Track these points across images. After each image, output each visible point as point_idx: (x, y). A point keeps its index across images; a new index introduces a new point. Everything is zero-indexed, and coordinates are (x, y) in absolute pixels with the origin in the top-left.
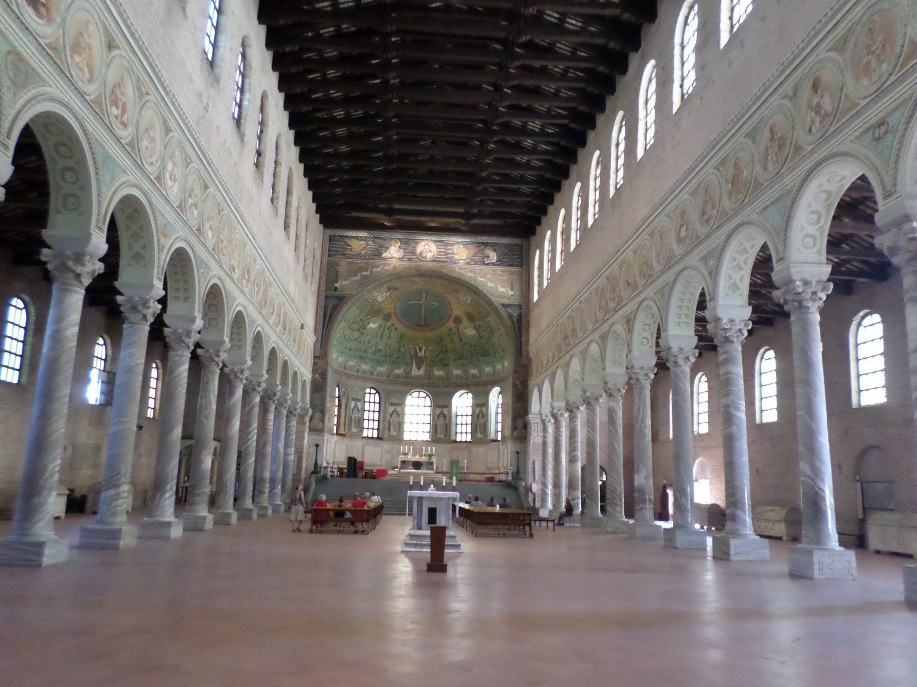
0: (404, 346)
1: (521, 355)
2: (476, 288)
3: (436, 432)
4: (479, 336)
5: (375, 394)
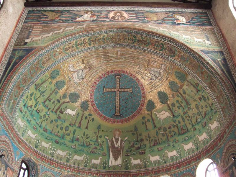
0: (101, 137)
2: (171, 39)
4: (174, 116)
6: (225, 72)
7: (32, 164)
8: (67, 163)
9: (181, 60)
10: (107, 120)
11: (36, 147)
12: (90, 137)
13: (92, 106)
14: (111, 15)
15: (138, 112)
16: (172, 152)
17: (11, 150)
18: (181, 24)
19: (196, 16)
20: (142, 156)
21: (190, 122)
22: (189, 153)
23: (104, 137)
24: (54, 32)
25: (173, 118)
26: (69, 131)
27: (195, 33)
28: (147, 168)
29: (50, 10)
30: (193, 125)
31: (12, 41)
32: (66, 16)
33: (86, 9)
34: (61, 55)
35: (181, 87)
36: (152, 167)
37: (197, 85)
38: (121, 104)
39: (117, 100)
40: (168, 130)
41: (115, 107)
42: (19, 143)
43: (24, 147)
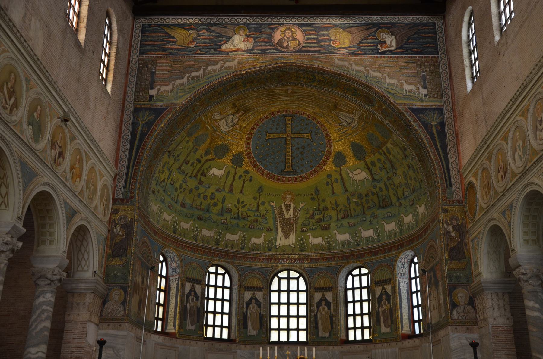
0: (263, 203)
1: (451, 186)
2: (367, 86)
3: (317, 328)
4: (373, 179)
5: (223, 275)
6: (439, 146)
7: (171, 255)
8: (217, 246)
9: (382, 114)
10: (273, 178)
12: (246, 205)
13: (249, 159)
14: (277, 36)
15: (321, 168)
16: (368, 231)
17: (150, 247)
18: (388, 52)
19: (415, 33)
20: (325, 232)
21: (395, 192)
22: (390, 236)
24: (190, 73)
25: (373, 181)
26: (215, 200)
27: (408, 71)
28: (332, 251)
29: (177, 23)
30: (398, 199)
31: (129, 92)
32: (204, 39)
33: (236, 23)
35: (385, 143)
36: (339, 249)
37: (405, 149)
38: (294, 155)
39: (287, 150)
40: (365, 198)
41: (284, 160)
42: (155, 235)
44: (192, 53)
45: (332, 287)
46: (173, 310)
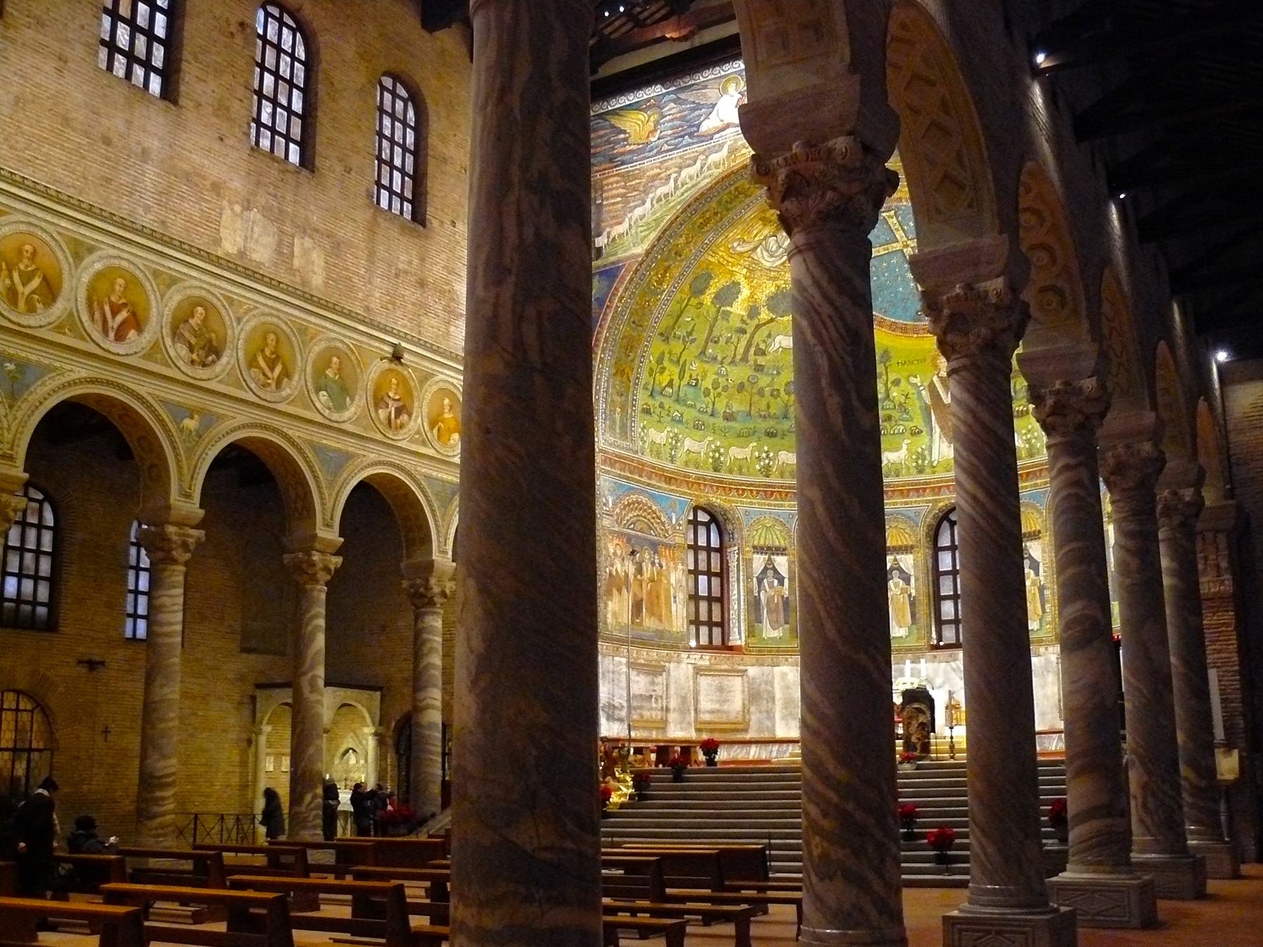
0: (897, 382)
10: (904, 330)
11: (716, 470)
23: (908, 380)
34: (695, 243)
43: (684, 484)
44: (655, 151)
45: (1039, 532)
46: (736, 607)
